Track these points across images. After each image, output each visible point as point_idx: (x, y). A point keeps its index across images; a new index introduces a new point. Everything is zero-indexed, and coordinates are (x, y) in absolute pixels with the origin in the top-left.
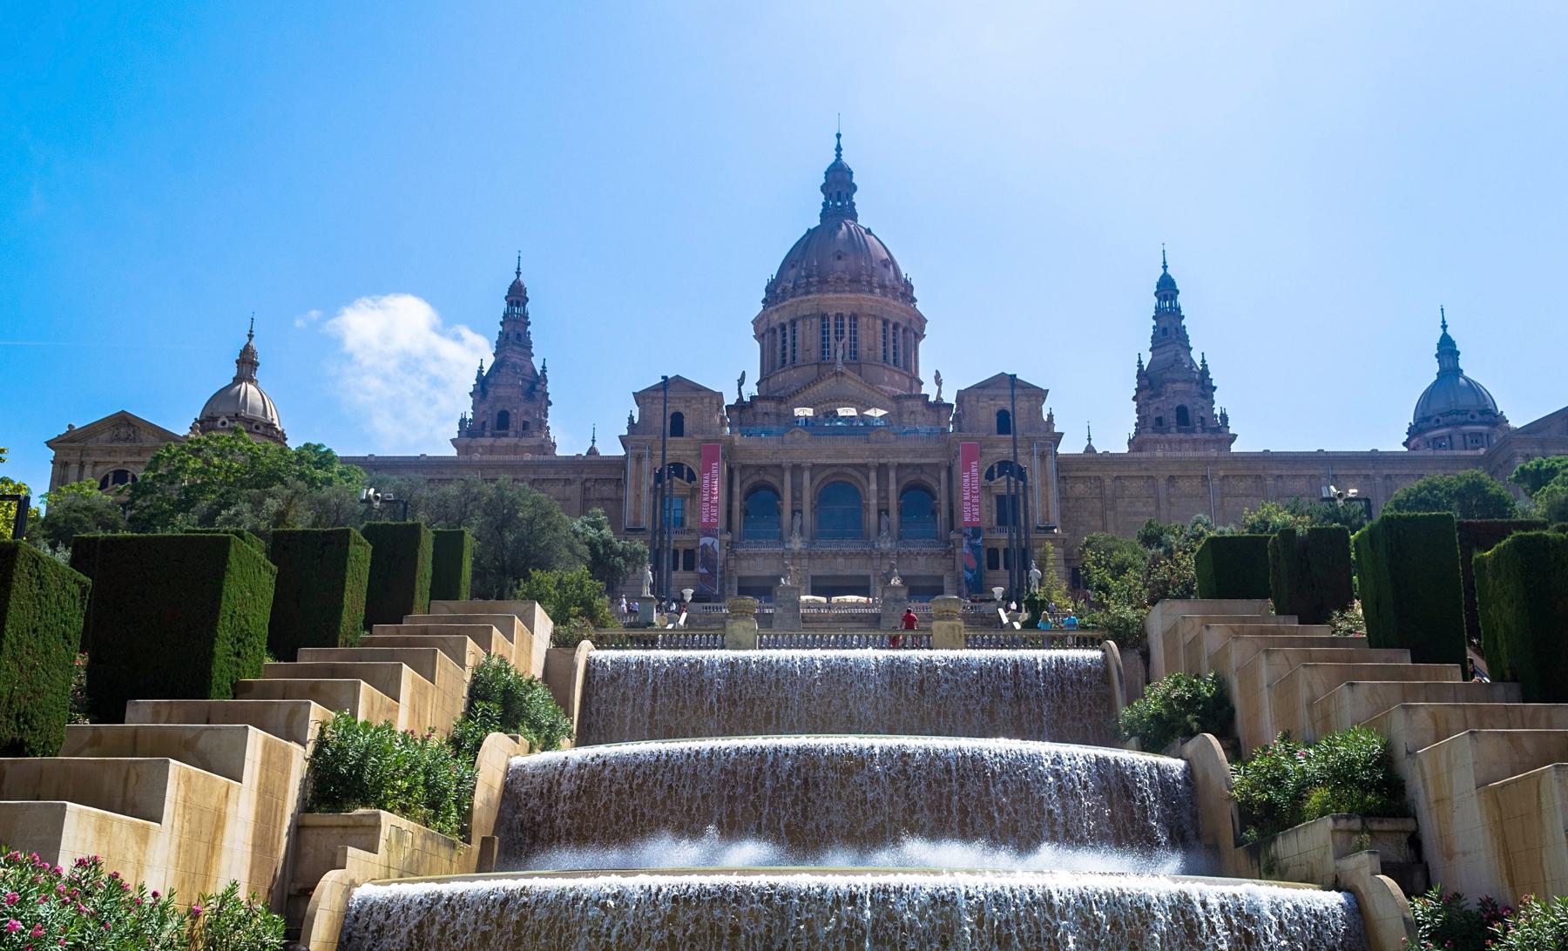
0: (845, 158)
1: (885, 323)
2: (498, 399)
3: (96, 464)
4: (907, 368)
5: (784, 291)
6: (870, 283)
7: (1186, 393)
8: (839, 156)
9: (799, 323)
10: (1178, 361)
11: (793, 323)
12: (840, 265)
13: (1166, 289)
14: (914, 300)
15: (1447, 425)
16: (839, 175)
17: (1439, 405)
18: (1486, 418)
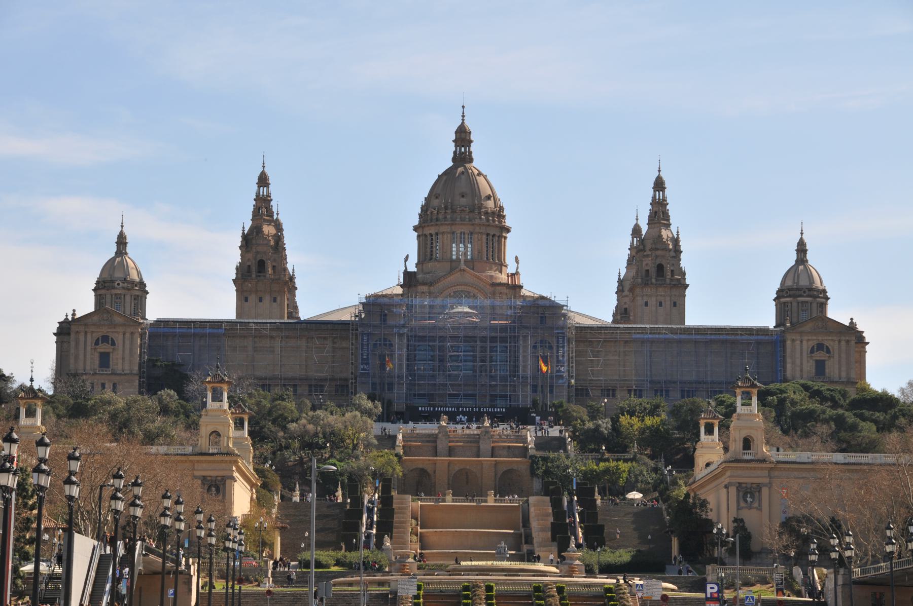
0: (467, 123)
1: (488, 235)
2: (258, 253)
3: (93, 332)
4: (500, 259)
5: (432, 212)
6: (480, 213)
7: (663, 256)
8: (463, 120)
9: (440, 236)
10: (660, 236)
11: (437, 234)
12: (463, 201)
13: (659, 185)
14: (504, 217)
15: (790, 296)
16: (463, 135)
17: (789, 283)
18: (811, 293)
